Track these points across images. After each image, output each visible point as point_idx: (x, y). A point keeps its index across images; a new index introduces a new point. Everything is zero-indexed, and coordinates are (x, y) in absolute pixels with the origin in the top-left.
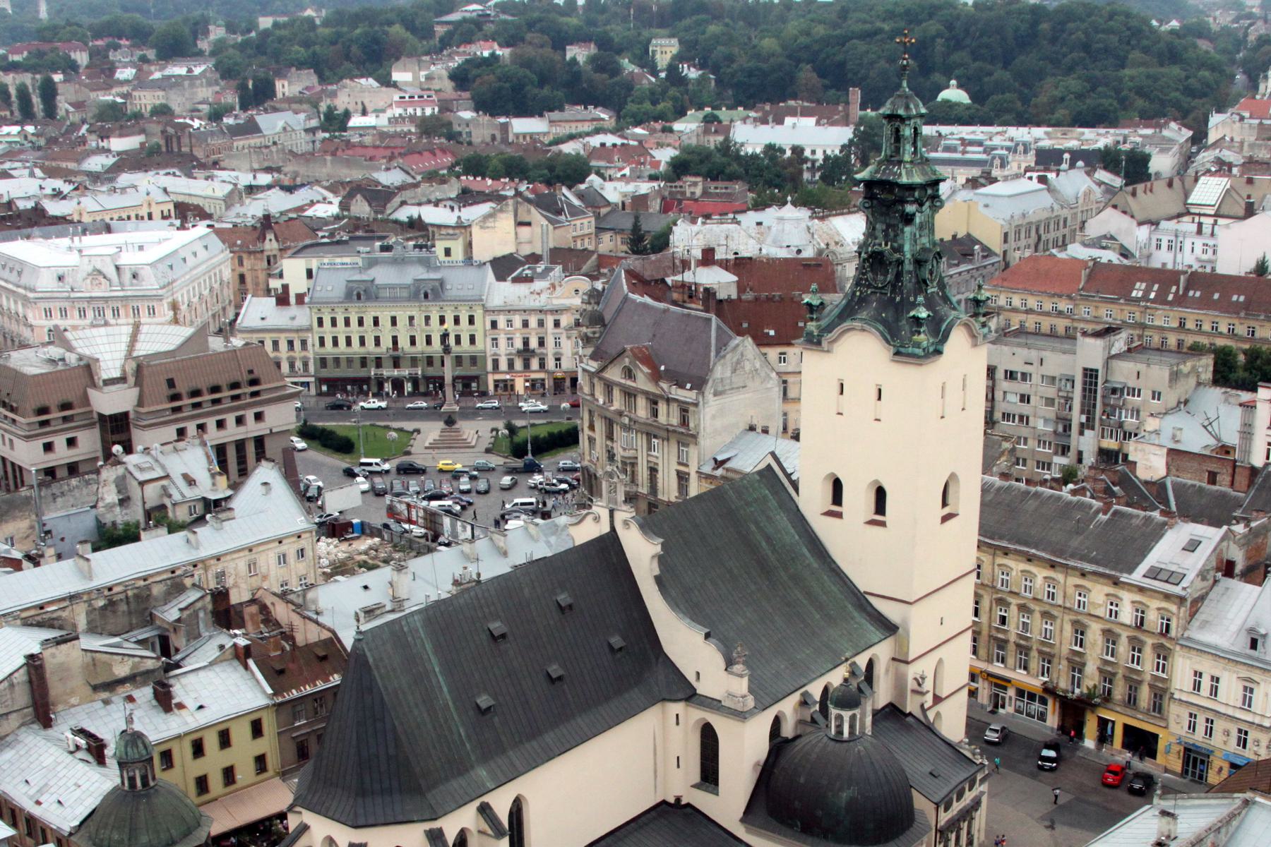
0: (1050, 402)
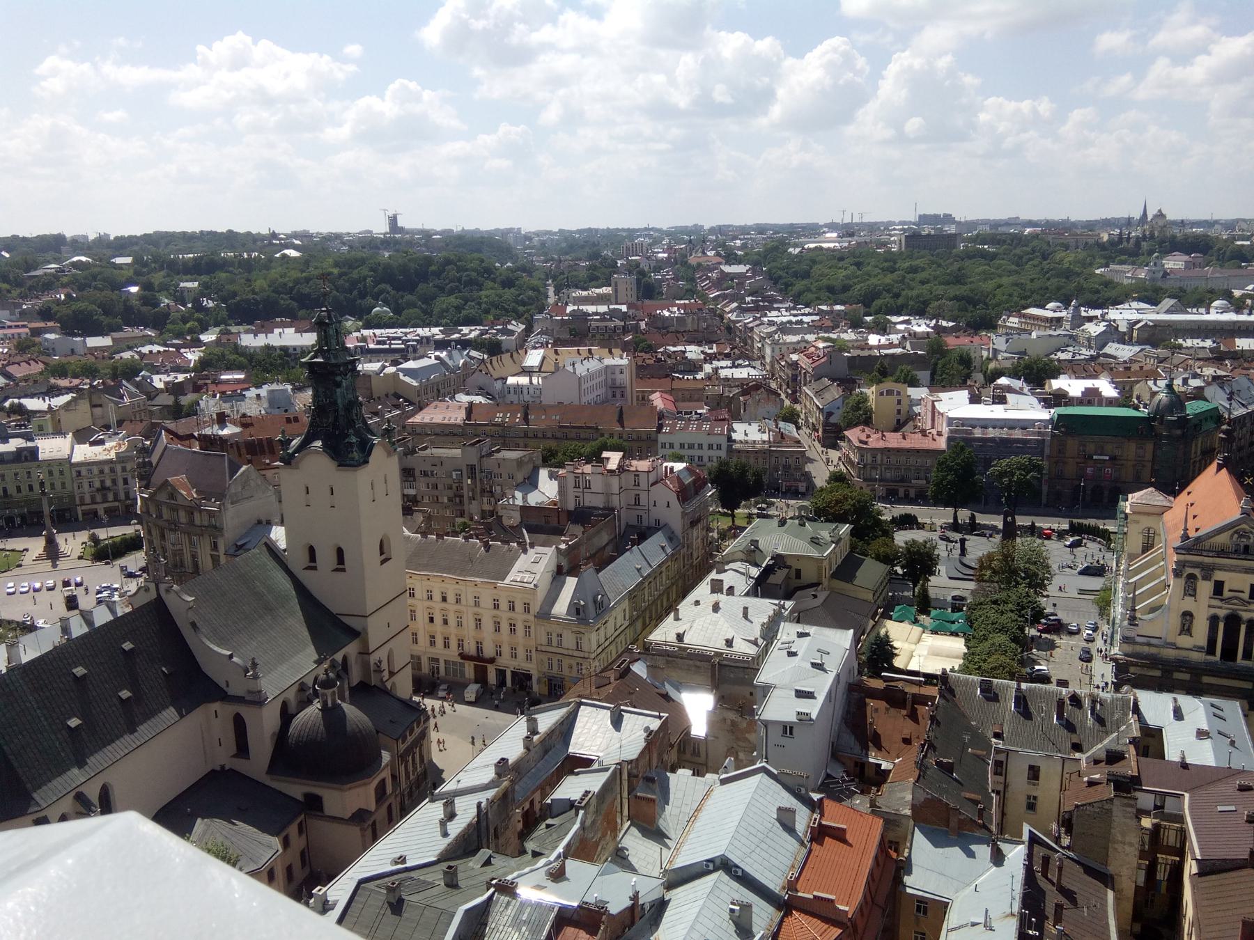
0: (450, 488)
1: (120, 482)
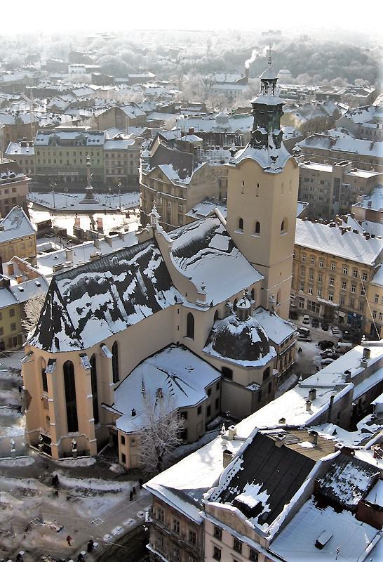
0: (321, 191)
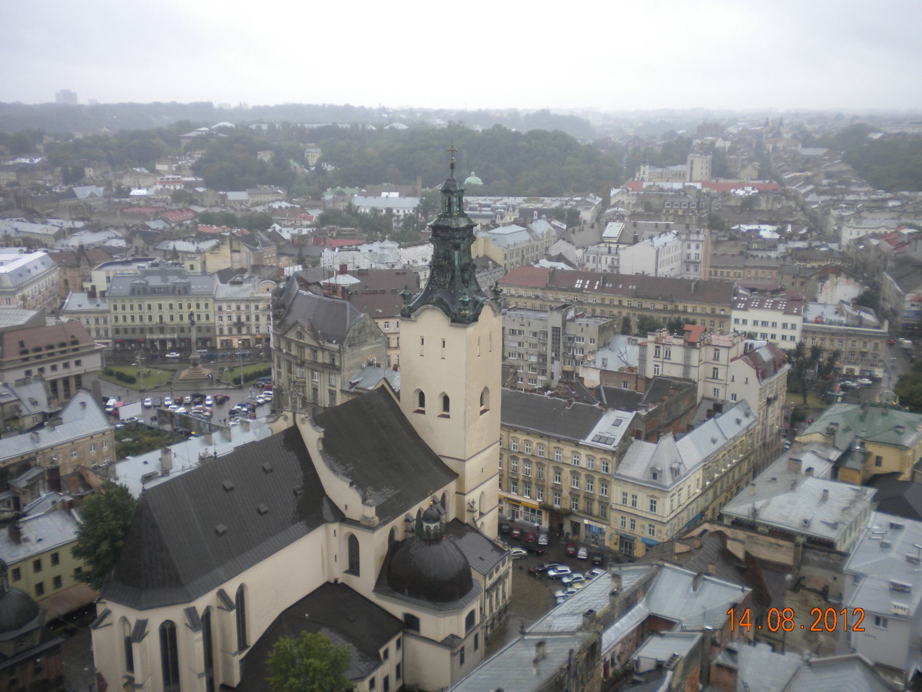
1: (253, 318)
